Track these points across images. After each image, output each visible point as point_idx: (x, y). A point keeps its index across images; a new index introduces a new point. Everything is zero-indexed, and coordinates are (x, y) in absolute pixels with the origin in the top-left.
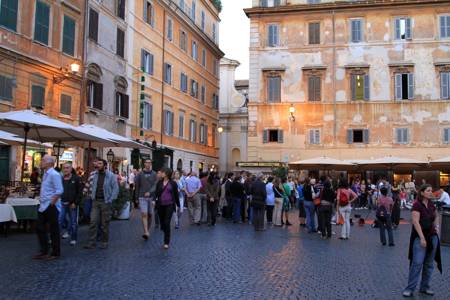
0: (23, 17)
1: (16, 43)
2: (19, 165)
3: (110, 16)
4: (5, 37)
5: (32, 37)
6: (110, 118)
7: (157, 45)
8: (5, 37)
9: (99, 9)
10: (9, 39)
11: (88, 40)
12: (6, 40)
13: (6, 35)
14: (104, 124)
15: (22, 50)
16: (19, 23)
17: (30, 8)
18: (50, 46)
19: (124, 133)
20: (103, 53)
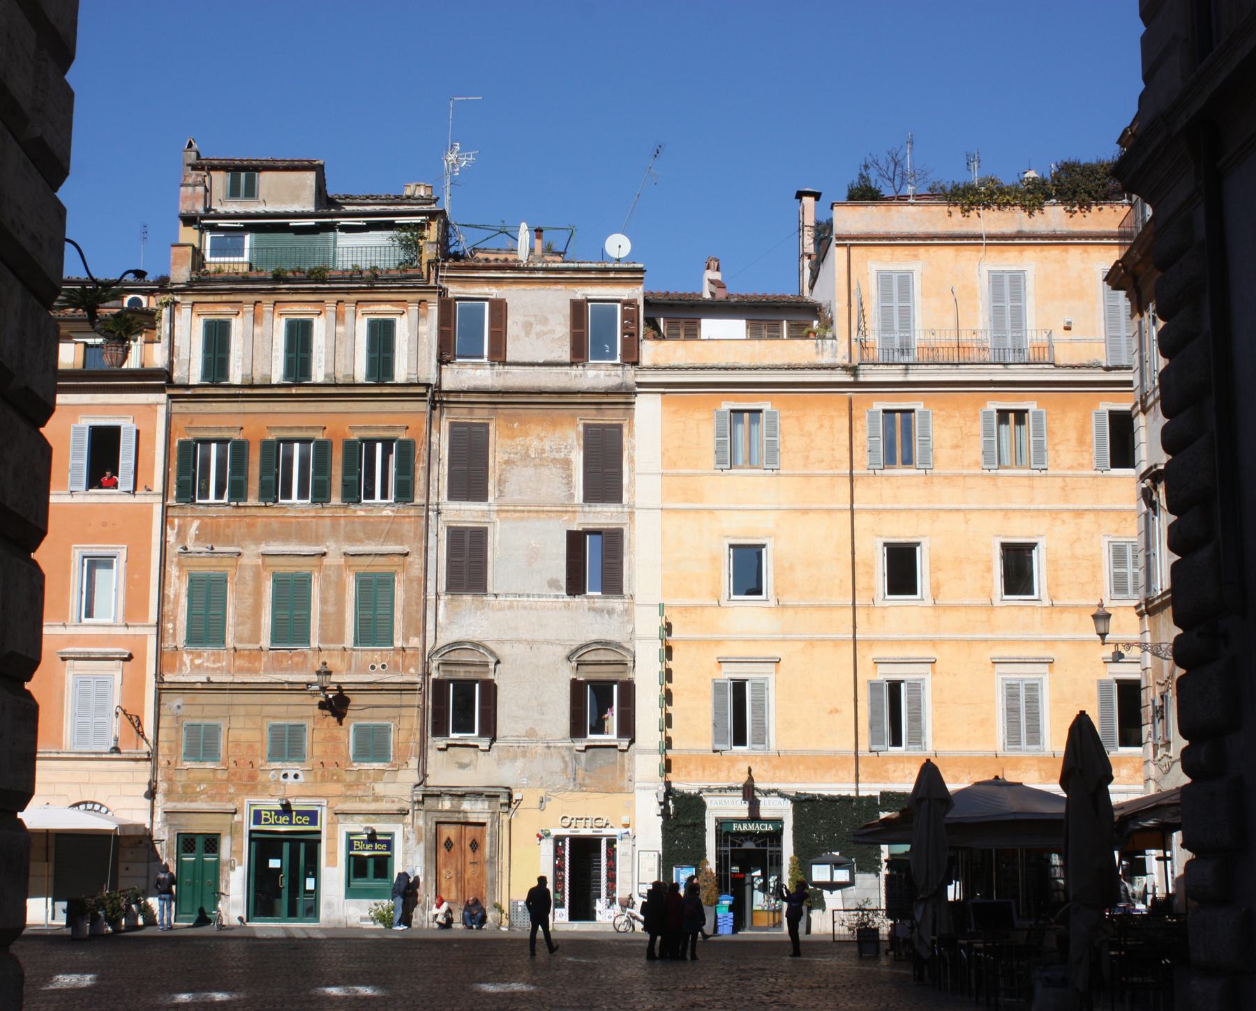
0: (238, 615)
1: (224, 663)
2: (240, 864)
3: (542, 516)
4: (198, 662)
5: (266, 642)
6: (549, 747)
7: (806, 511)
8: (198, 662)
9: (494, 516)
10: (208, 660)
11: (444, 599)
12: (199, 666)
13: (199, 656)
14: (520, 763)
15: (241, 670)
16: (230, 628)
17: (258, 593)
18: (315, 643)
19: (627, 775)
20: (511, 607)
